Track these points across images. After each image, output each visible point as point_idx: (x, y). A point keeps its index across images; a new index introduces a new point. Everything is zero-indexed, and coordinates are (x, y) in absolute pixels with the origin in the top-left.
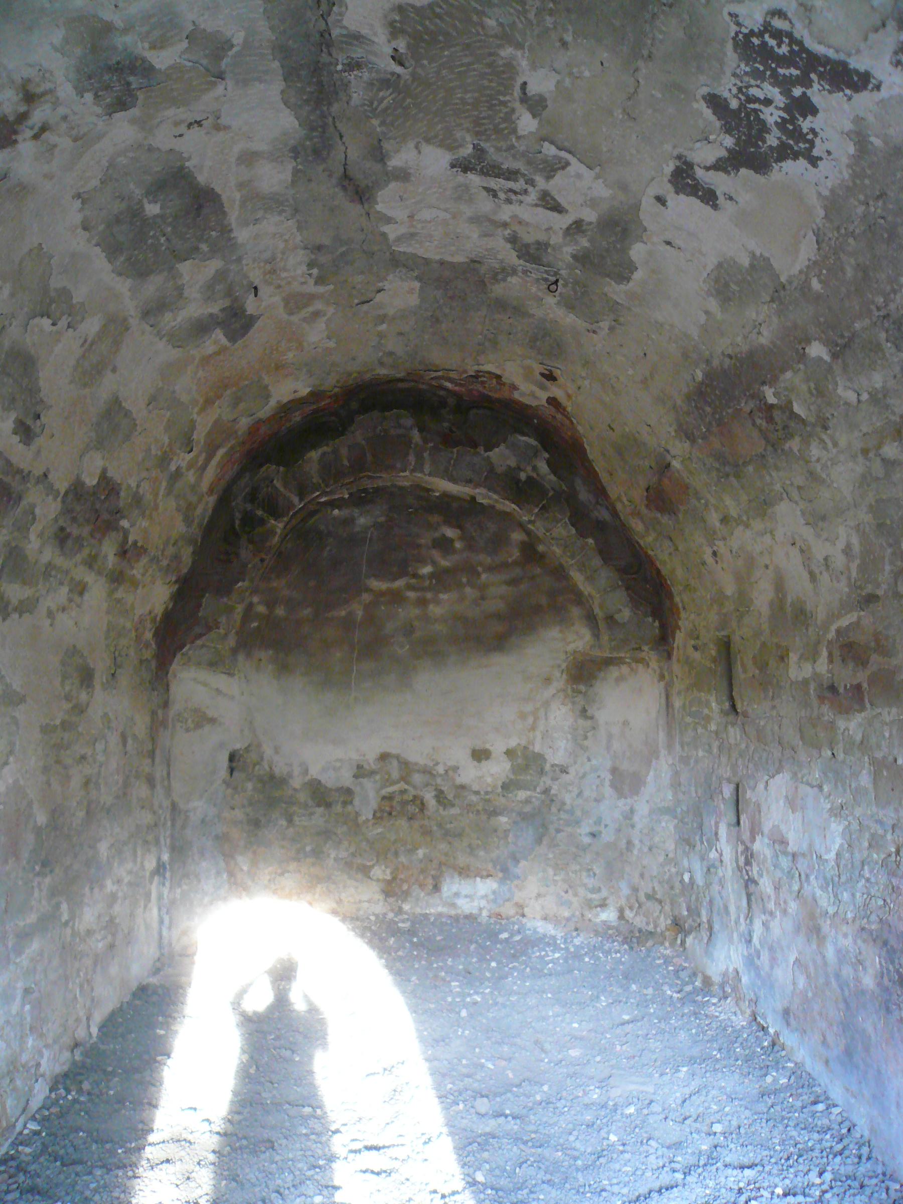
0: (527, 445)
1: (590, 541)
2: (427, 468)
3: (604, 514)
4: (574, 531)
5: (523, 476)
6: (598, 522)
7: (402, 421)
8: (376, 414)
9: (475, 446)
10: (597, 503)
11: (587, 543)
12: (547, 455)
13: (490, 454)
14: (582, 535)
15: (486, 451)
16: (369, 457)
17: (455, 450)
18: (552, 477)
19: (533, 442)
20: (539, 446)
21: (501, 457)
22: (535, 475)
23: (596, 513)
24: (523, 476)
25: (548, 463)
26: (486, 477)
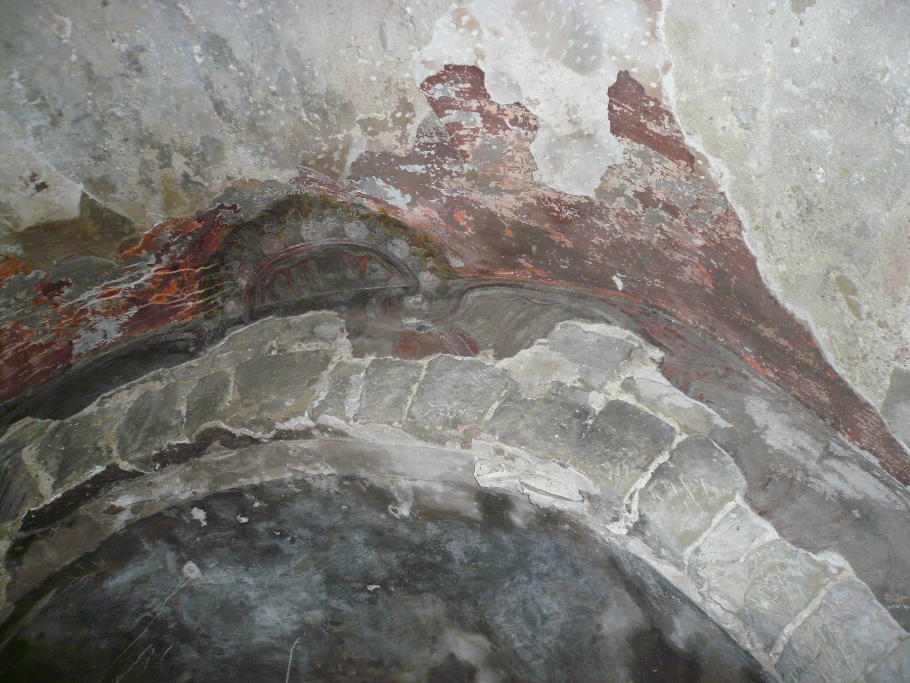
0: (605, 343)
1: (834, 559)
2: (353, 403)
3: (857, 482)
4: (771, 533)
5: (596, 402)
6: (845, 504)
7: (321, 329)
8: (271, 321)
9: (474, 349)
10: (828, 454)
11: (824, 567)
12: (658, 354)
13: (505, 363)
14: (803, 538)
15: (499, 357)
16: (231, 395)
17: (424, 362)
18: (683, 401)
19: (616, 332)
20: (637, 340)
21: (538, 365)
22: (628, 399)
23: (832, 480)
24: (596, 402)
25: (662, 366)
26: (499, 412)
